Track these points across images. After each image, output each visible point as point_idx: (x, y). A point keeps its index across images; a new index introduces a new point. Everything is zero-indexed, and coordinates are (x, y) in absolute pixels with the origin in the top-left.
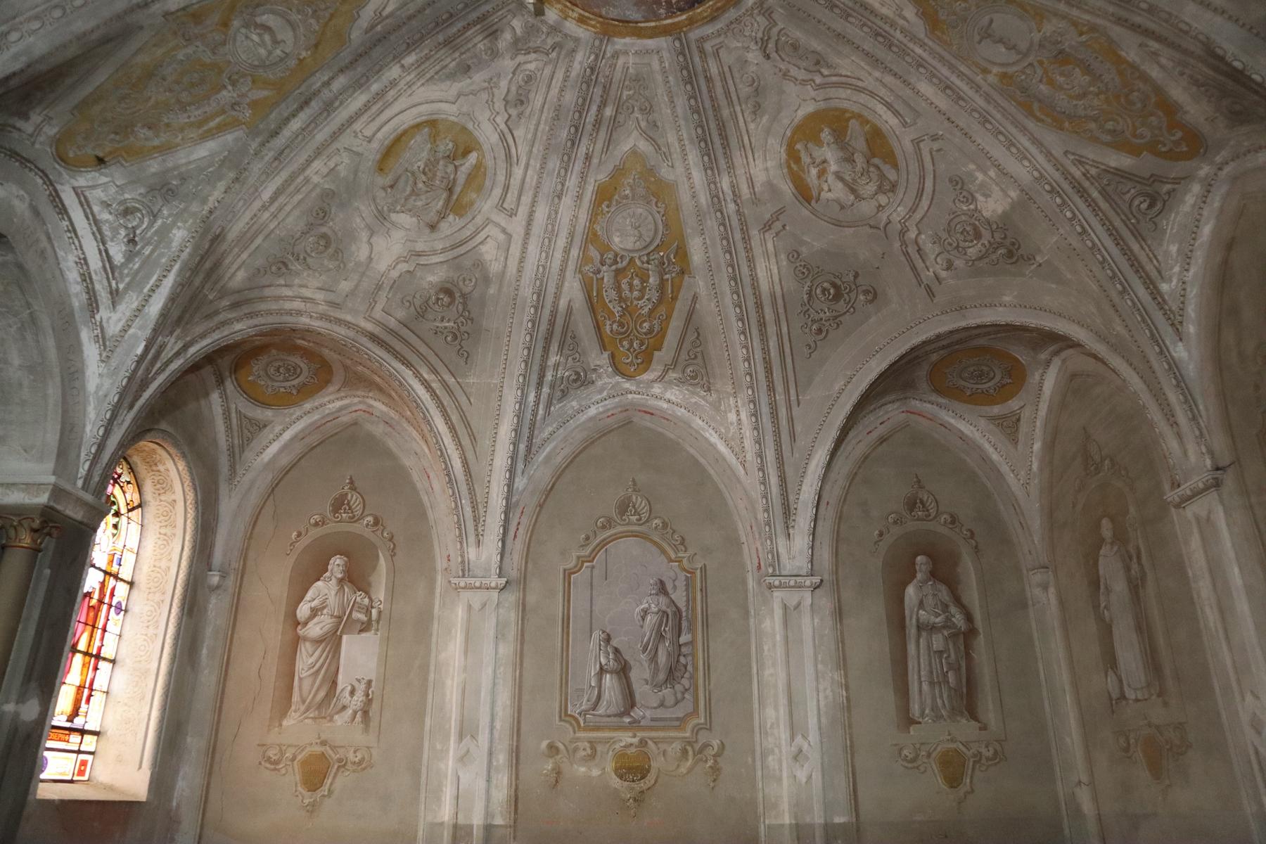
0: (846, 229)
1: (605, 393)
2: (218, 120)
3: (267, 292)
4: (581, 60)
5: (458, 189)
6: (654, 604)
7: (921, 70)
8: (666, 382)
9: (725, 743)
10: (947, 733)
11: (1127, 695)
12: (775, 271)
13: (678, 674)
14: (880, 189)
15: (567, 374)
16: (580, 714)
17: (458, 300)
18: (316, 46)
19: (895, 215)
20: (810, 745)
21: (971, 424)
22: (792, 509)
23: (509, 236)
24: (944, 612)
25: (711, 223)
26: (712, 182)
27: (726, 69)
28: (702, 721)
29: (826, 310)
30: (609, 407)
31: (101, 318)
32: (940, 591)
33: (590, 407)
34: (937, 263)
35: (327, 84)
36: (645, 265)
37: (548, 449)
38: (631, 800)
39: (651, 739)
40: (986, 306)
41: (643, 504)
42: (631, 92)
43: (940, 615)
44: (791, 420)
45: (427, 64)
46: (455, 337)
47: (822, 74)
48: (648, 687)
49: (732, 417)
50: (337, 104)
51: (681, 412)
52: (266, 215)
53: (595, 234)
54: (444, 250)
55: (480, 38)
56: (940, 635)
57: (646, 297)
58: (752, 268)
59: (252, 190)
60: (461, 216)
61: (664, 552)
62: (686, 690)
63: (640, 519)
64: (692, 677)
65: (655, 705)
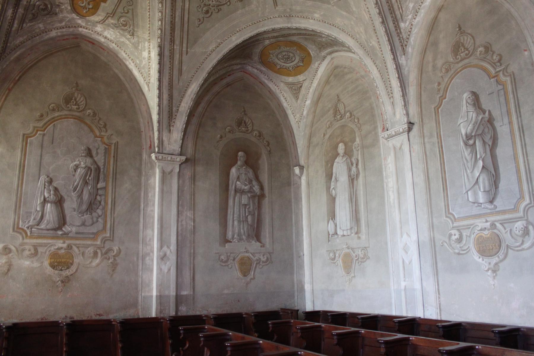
1: (64, 24)
6: (84, 162)
8: (105, 25)
9: (120, 247)
10: (244, 248)
11: (338, 233)
13: (95, 206)
16: (28, 228)
20: (171, 251)
21: (276, 85)
22: (174, 115)
24: (249, 184)
28: (108, 235)
30: (65, 33)
32: (248, 172)
33: (51, 30)
38: (59, 282)
39: (75, 245)
40: (304, 17)
41: (82, 99)
43: (247, 185)
44: (181, 63)
48: (75, 213)
49: (145, 54)
51: (113, 46)
56: (246, 196)
61: (92, 131)
62: (99, 216)
63: (79, 108)
64: (104, 208)
65: (79, 224)
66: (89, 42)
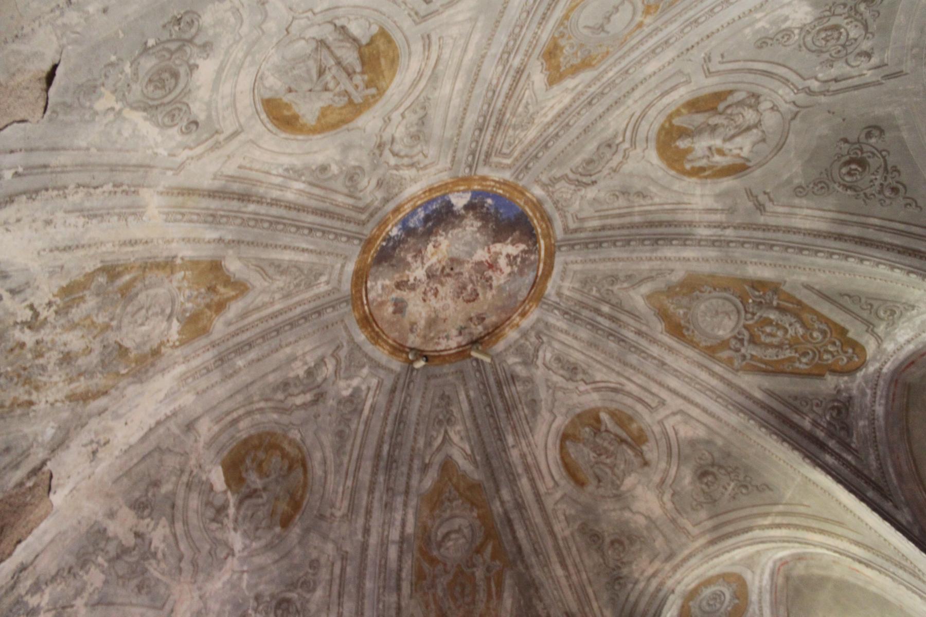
0: (788, 141)
1: (869, 391)
2: (493, 585)
3: (632, 599)
4: (555, 320)
5: (624, 435)
7: (631, 71)
12: (809, 212)
14: (755, 107)
15: (828, 418)
17: (715, 470)
18: (473, 504)
19: (787, 98)
23: (681, 412)
25: (738, 253)
26: (699, 243)
27: (597, 214)
29: (873, 177)
30: (884, 393)
33: (874, 411)
34: (858, 66)
35: (502, 503)
36: (756, 318)
37: (891, 470)
42: (594, 289)
45: (518, 428)
46: (746, 487)
47: (621, 143)
50: (520, 500)
52: (574, 578)
53: (707, 348)
54: (669, 463)
55: (513, 388)
57: (787, 326)
58: (797, 231)
59: (550, 581)
60: (646, 440)
66: (908, 367)
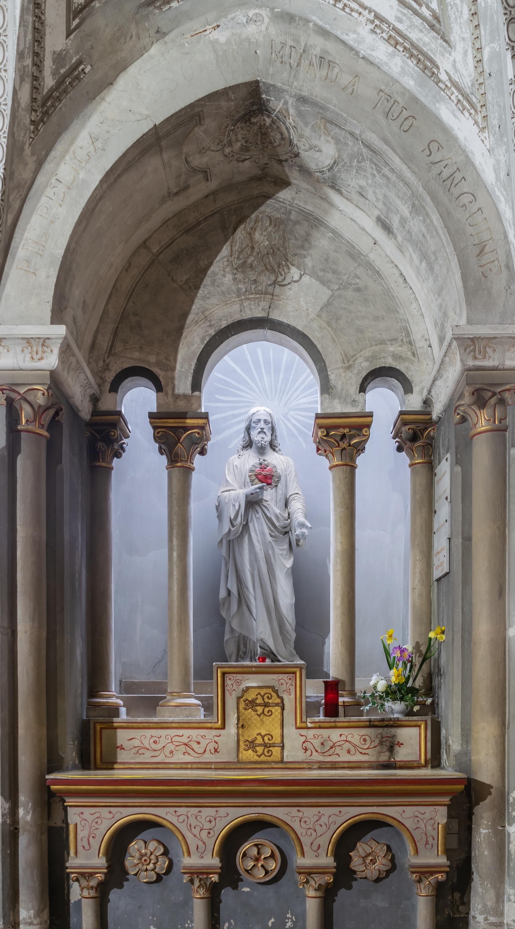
31: (447, 73)
